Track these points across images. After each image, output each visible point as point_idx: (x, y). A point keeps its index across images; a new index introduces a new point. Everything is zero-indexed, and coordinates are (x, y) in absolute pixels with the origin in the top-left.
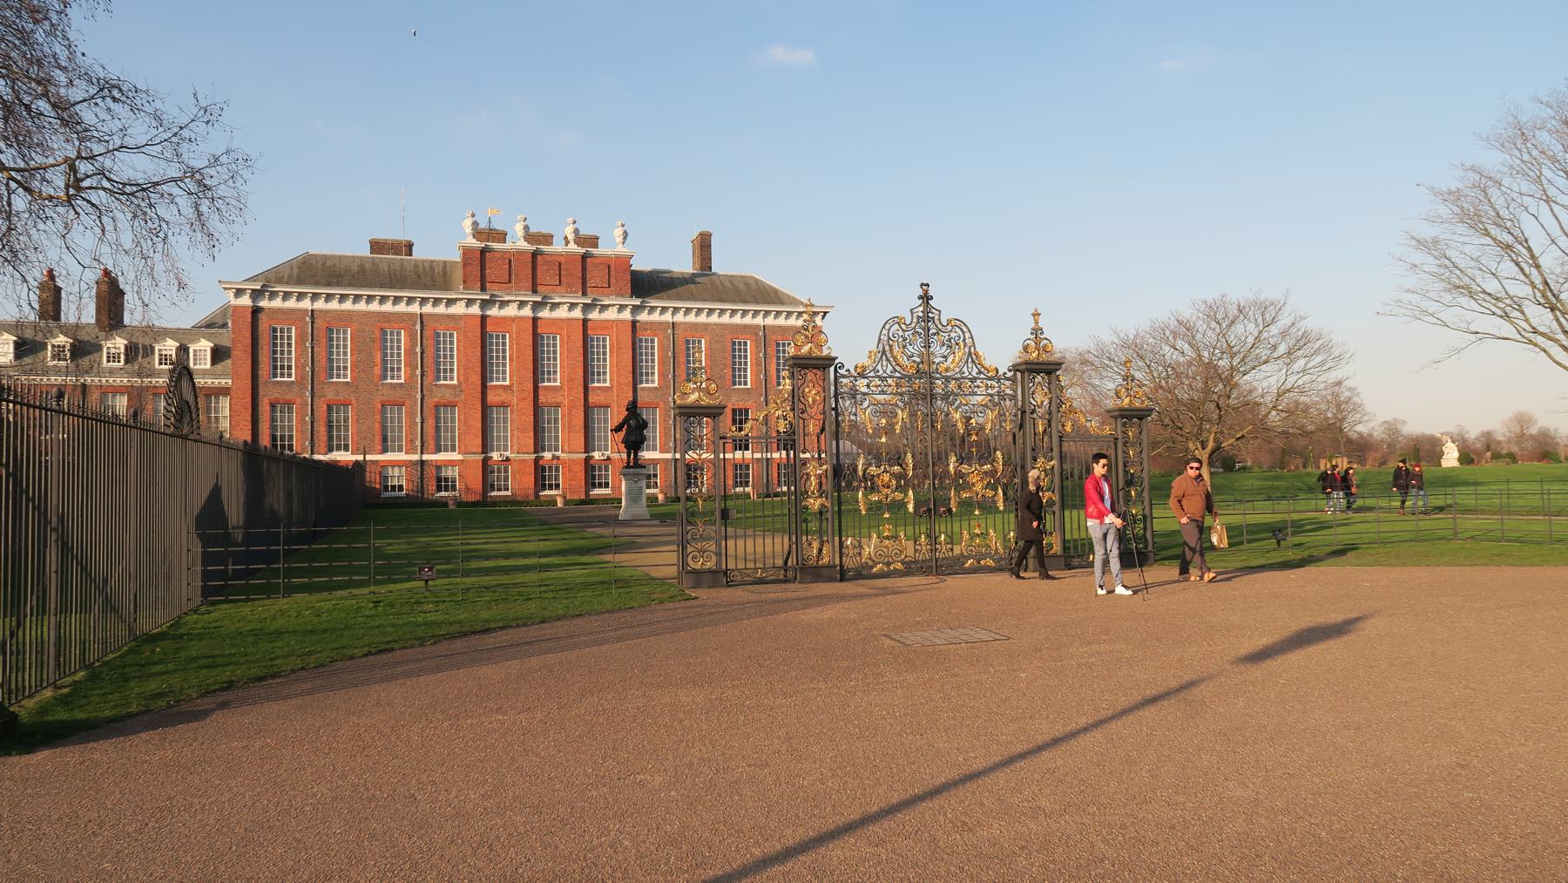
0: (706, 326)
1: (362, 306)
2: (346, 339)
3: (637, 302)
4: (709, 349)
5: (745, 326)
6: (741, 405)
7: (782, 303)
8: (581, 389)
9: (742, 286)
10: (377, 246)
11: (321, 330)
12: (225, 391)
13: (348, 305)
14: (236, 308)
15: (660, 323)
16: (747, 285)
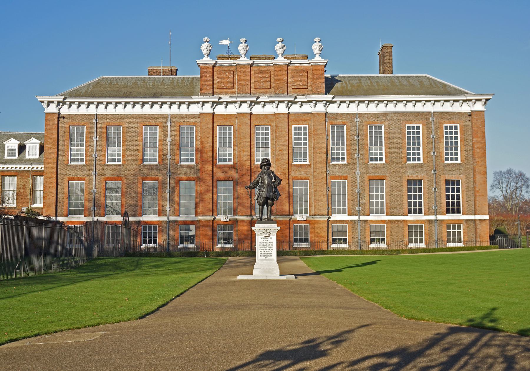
0: (385, 114)
1: (129, 109)
2: (116, 132)
3: (329, 98)
4: (388, 133)
5: (419, 114)
6: (414, 177)
7: (449, 93)
8: (286, 166)
9: (416, 84)
10: (151, 72)
11: (98, 125)
12: (40, 174)
13: (120, 109)
14: (48, 115)
15: (348, 114)
16: (421, 83)
